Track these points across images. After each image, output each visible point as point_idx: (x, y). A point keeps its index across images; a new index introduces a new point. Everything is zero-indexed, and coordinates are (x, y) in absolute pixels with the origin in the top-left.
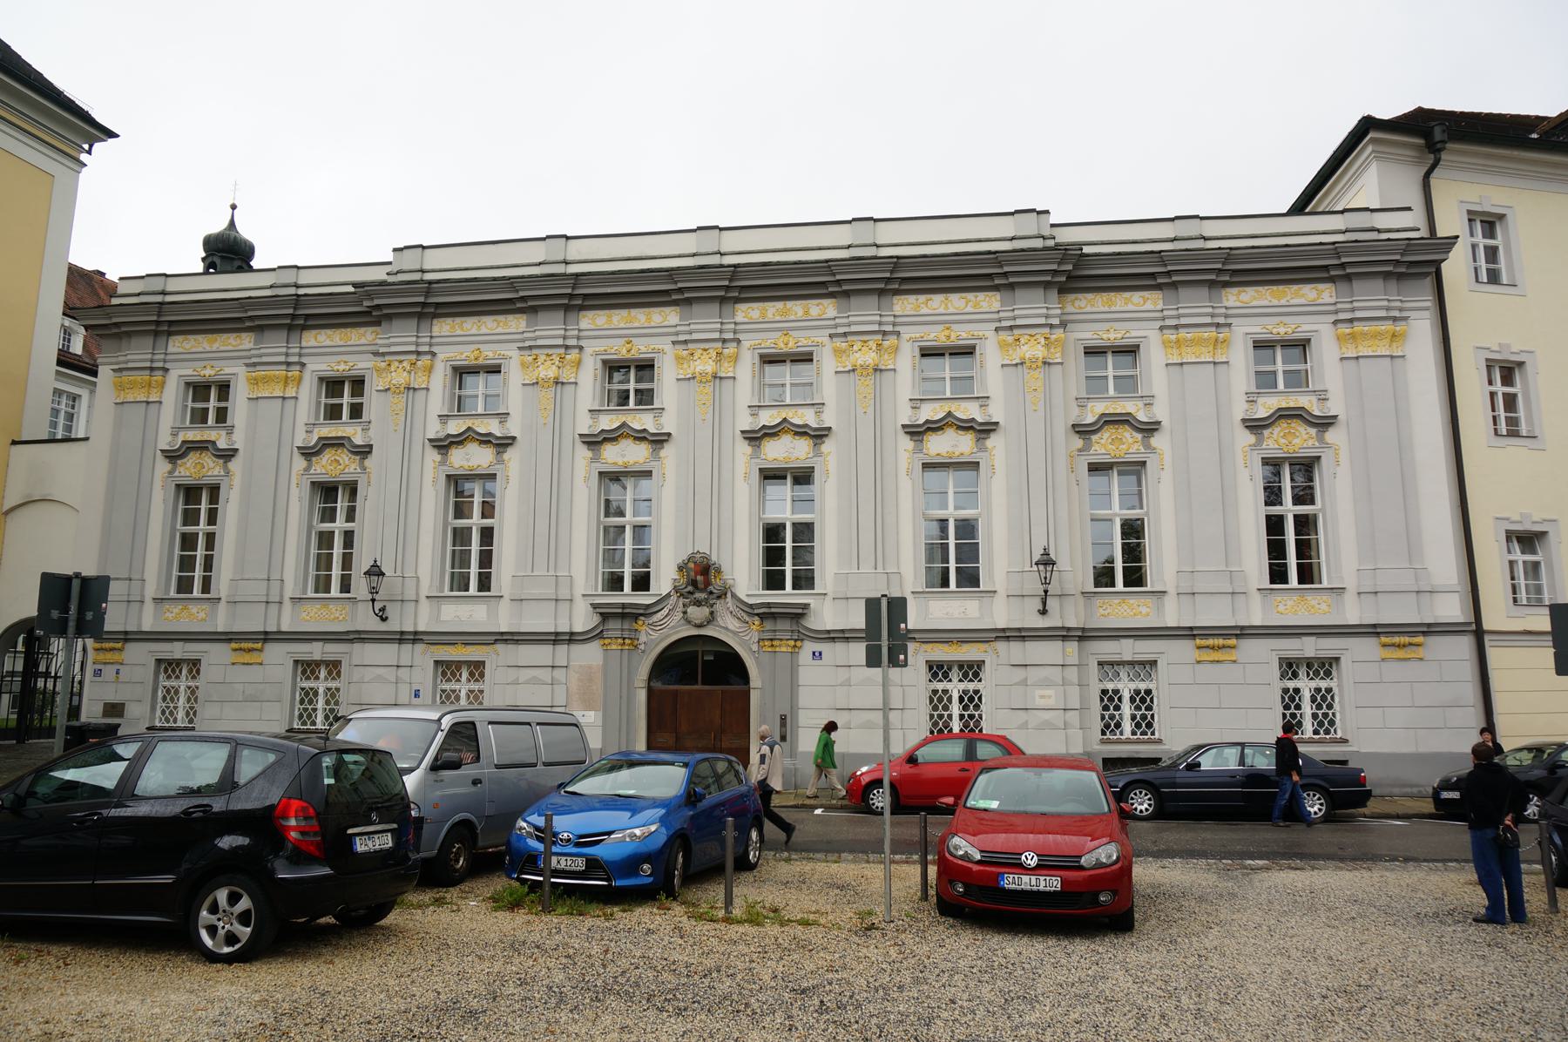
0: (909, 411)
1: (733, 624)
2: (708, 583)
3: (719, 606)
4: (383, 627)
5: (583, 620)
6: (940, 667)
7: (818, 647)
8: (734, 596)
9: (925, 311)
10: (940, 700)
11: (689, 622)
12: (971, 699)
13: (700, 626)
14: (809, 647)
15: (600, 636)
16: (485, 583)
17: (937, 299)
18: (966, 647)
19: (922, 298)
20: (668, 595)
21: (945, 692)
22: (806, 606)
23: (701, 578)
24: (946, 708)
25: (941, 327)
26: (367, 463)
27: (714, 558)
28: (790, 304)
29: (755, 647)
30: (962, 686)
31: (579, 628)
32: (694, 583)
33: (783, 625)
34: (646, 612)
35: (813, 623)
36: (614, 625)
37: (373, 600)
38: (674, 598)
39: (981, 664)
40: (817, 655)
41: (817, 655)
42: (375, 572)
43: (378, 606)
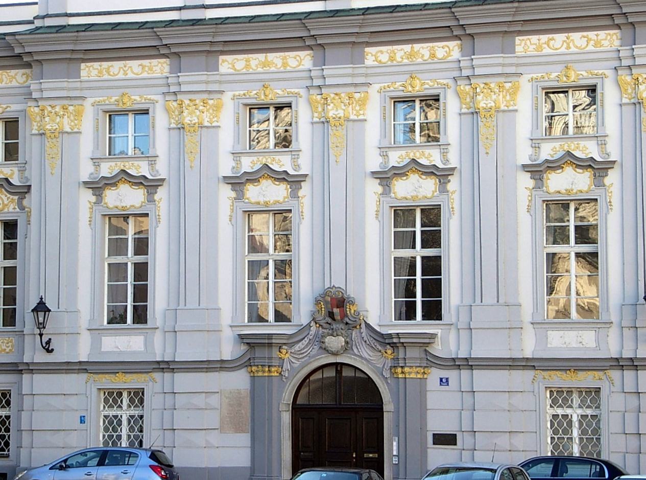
0: (530, 151)
1: (366, 352)
2: (344, 315)
3: (354, 333)
4: (49, 358)
5: (228, 350)
6: (560, 392)
7: (444, 374)
8: (368, 326)
9: (547, 51)
10: (560, 424)
11: (326, 350)
12: (560, 424)
13: (335, 354)
14: (435, 374)
15: (248, 364)
16: (141, 316)
17: (560, 37)
18: (581, 375)
19: (544, 38)
20: (309, 325)
21: (565, 416)
22: (433, 336)
23: (336, 309)
24: (565, 432)
25: (561, 67)
26: (25, 202)
27: (351, 292)
28: (417, 46)
29: (387, 374)
30: (580, 411)
31: (227, 356)
32: (331, 315)
33: (413, 353)
34: (290, 341)
35: (438, 349)
36: (259, 352)
37: (41, 335)
38: (314, 328)
39: (598, 390)
40: (444, 382)
41: (444, 382)
42: (41, 307)
43: (45, 339)
